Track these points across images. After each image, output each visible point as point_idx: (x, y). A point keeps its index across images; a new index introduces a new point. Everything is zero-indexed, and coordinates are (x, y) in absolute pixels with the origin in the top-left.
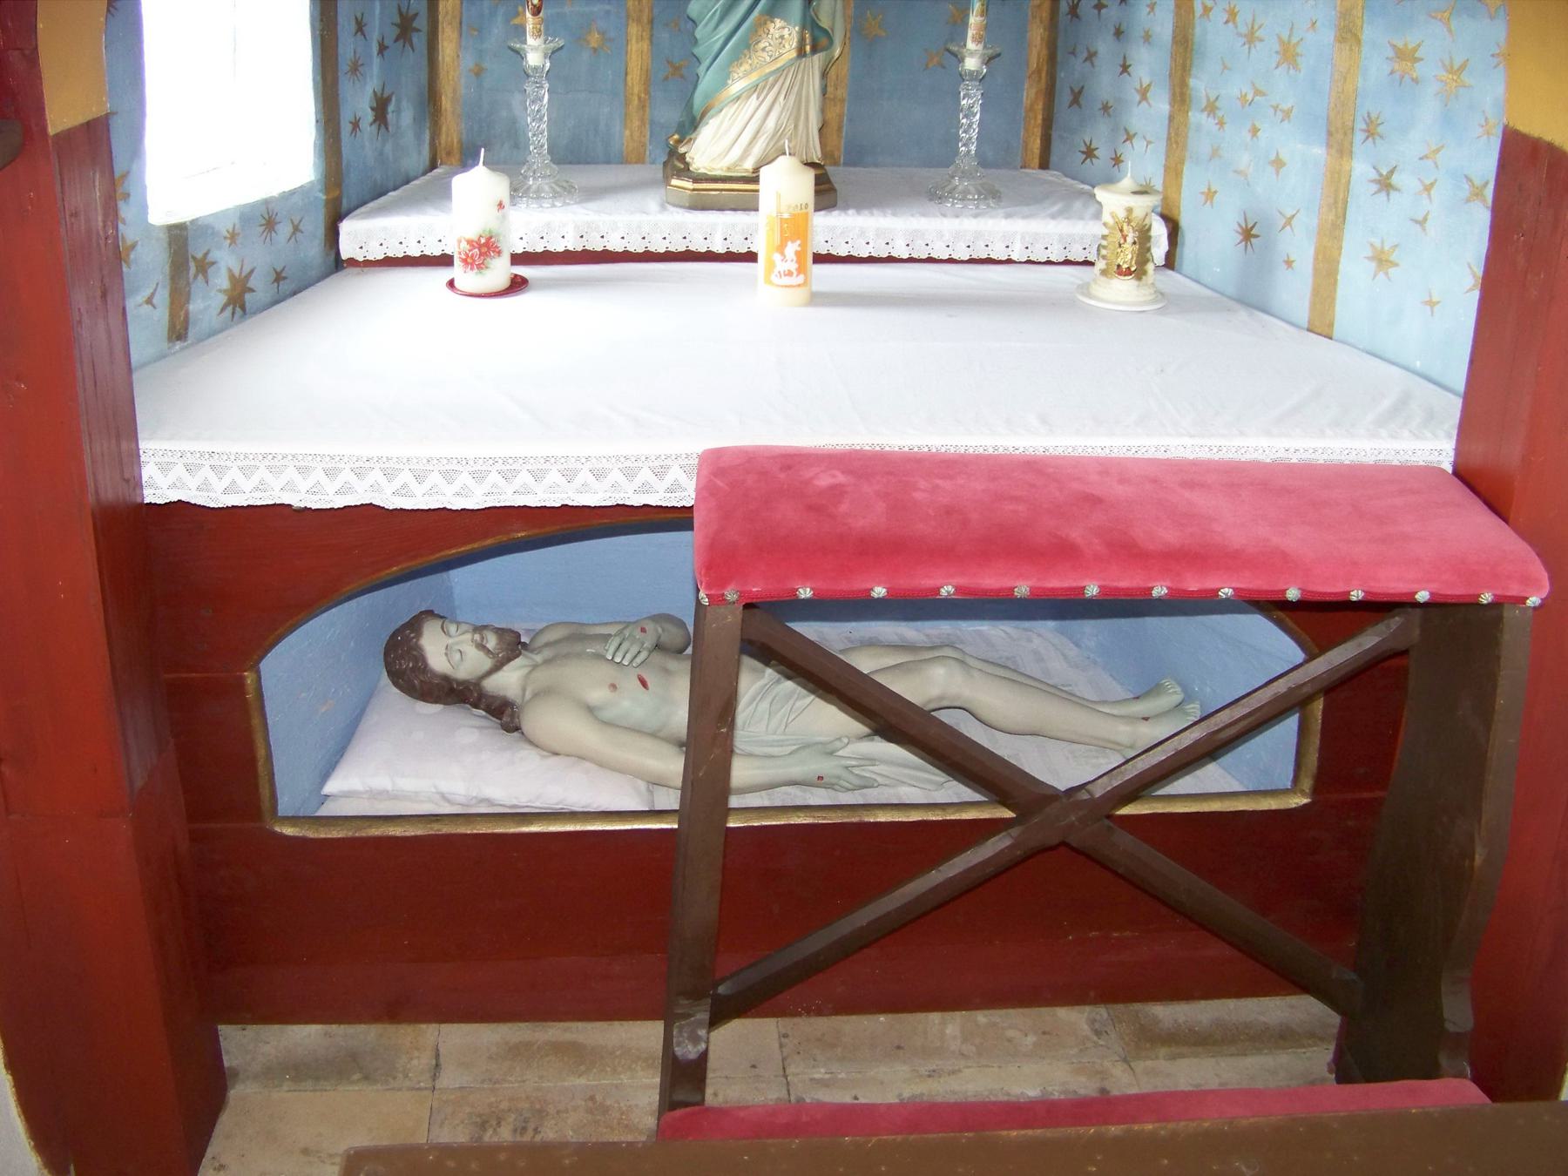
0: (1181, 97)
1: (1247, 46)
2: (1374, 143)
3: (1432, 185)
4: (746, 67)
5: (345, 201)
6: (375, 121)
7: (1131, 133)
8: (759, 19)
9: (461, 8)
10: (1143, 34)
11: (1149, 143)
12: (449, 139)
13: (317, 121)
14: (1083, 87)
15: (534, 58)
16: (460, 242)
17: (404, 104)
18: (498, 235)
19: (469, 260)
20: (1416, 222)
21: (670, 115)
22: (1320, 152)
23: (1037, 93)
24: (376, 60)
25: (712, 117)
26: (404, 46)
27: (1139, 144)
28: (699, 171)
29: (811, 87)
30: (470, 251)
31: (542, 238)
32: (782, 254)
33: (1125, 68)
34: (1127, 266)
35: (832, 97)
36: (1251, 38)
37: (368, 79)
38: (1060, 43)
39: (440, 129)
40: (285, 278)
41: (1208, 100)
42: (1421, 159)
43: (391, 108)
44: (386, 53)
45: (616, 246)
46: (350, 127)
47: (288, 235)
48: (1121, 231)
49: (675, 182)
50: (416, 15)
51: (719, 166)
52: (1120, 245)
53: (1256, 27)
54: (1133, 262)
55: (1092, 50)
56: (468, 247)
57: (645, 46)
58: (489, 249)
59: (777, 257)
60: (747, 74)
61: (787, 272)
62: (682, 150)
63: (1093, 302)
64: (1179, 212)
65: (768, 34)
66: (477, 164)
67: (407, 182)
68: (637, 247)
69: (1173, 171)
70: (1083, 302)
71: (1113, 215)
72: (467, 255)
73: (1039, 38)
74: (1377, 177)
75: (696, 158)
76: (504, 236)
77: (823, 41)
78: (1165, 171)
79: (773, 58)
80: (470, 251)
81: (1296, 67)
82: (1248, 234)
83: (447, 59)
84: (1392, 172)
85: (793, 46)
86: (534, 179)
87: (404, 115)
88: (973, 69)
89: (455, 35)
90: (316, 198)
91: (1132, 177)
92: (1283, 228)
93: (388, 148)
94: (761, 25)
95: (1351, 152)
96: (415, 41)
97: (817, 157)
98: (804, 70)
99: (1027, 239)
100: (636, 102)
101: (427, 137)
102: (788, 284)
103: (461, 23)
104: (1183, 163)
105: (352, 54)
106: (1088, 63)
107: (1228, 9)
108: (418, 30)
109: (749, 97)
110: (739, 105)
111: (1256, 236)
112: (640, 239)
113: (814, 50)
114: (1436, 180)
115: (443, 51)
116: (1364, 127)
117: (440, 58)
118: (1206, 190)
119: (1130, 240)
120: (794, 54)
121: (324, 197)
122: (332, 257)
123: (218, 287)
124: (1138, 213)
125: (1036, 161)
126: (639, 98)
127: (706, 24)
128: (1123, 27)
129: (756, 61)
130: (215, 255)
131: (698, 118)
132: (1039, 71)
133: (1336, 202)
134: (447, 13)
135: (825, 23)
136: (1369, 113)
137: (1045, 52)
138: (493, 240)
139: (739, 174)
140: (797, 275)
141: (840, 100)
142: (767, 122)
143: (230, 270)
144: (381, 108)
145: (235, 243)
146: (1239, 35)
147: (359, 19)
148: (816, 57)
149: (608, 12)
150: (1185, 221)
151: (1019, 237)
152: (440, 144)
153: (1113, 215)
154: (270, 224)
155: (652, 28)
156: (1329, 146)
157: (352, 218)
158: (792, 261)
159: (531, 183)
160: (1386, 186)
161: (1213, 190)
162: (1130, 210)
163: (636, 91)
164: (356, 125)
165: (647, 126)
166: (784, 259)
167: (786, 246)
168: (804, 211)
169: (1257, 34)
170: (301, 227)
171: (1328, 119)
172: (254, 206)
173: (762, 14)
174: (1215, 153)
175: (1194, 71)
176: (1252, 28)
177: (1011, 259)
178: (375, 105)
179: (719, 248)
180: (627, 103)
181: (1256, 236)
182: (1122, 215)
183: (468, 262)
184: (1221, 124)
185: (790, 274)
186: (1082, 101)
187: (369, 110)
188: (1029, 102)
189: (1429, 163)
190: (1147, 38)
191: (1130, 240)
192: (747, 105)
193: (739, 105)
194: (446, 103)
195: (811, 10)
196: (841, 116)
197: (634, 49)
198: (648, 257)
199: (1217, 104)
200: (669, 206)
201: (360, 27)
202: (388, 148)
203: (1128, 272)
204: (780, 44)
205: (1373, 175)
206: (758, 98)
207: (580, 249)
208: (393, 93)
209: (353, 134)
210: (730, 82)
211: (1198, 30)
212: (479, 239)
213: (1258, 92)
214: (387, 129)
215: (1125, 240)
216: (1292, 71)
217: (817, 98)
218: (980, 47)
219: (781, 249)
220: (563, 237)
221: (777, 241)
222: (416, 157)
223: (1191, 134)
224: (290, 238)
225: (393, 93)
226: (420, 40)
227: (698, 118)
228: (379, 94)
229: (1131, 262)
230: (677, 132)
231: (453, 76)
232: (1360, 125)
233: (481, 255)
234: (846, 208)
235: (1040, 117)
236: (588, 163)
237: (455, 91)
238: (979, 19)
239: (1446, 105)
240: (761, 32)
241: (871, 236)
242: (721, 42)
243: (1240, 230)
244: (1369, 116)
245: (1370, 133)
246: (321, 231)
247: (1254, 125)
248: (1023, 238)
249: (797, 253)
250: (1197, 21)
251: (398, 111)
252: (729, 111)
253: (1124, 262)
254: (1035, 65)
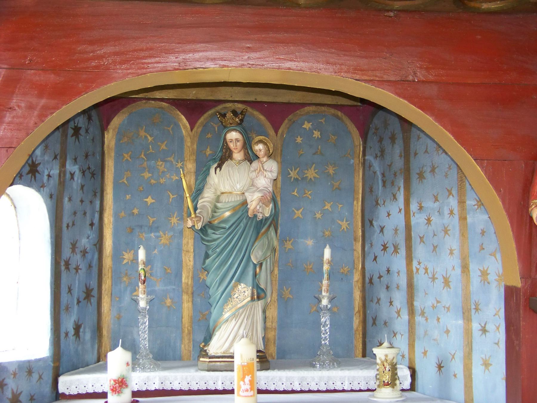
0: (412, 312)
1: (432, 282)
2: (478, 313)
3: (499, 326)
4: (230, 306)
5: (61, 369)
6: (74, 335)
7: (395, 333)
8: (235, 284)
9: (112, 287)
10: (396, 286)
11: (402, 335)
12: (106, 349)
13: (51, 329)
14: (376, 316)
15: (142, 304)
16: (110, 381)
17: (87, 330)
18: (126, 378)
19: (114, 389)
20: (496, 344)
21: (200, 337)
22: (461, 322)
23: (359, 322)
24: (76, 307)
25: (217, 332)
26: (87, 302)
27: (398, 336)
28: (212, 355)
29: (258, 316)
30: (115, 385)
31: (145, 384)
32: (244, 381)
33: (391, 303)
34: (387, 381)
35: (271, 327)
36: (434, 278)
37: (72, 314)
38: (367, 297)
39: (102, 344)
40: (34, 399)
41: (421, 310)
42: (494, 316)
43: (81, 330)
44: (80, 304)
45: (177, 387)
46: (64, 335)
47: (37, 379)
48: (384, 365)
49: (201, 359)
50: (93, 289)
51: (220, 352)
52: (384, 372)
53: (435, 273)
54: (390, 379)
55: (379, 298)
56: (114, 383)
57: (190, 304)
58: (123, 384)
59: (242, 383)
60: (230, 309)
61: (246, 390)
62: (205, 348)
63: (375, 399)
64: (415, 364)
65: (238, 291)
66: (118, 346)
67: (88, 366)
68: (185, 388)
69: (411, 346)
70: (372, 400)
71: (380, 359)
72: (113, 387)
73: (358, 296)
74: (481, 328)
75: (211, 350)
76: (129, 379)
77: (262, 294)
78: (409, 346)
79: (241, 301)
80: (115, 385)
81: (450, 288)
82: (440, 367)
83: (105, 311)
84: (485, 324)
85: (249, 296)
86: (143, 360)
87: (87, 335)
88: (325, 304)
89: (109, 300)
90: (49, 364)
91: (388, 341)
92: (452, 360)
93: (80, 348)
94: (235, 286)
95: (471, 319)
96: (92, 301)
97: (262, 349)
98: (254, 308)
99: (350, 380)
100: (186, 331)
101: (96, 346)
102: (247, 395)
103: (111, 294)
104: (415, 341)
105: (66, 302)
106: (378, 304)
107: (424, 267)
108: (94, 297)
109: (232, 320)
110: (228, 325)
111: (443, 367)
112: (187, 384)
113: (259, 298)
114: (500, 324)
115: (104, 307)
116: (474, 307)
117: (103, 311)
118: (424, 351)
119: (387, 369)
120: (249, 299)
121: (53, 365)
123: (7, 397)
124: (390, 357)
125: (361, 355)
126: (188, 329)
127: (213, 287)
128: (389, 285)
129: (234, 303)
130: (7, 381)
131: (212, 333)
132: (359, 312)
133: (468, 343)
134: (106, 290)
135: (262, 286)
136: (475, 301)
137: (361, 303)
138: (124, 380)
139: (228, 355)
140: (251, 391)
141: (274, 328)
142: (239, 331)
143: (12, 390)
144: (77, 328)
145: (15, 377)
146: (430, 278)
147: (70, 287)
148: (260, 302)
149: (174, 289)
150: (417, 368)
151: (347, 378)
152: (102, 351)
153: (380, 359)
154: (30, 372)
155: (193, 297)
156: (464, 319)
157: (64, 375)
158: (248, 384)
159: (141, 361)
160: (484, 331)
161: (426, 350)
162: (386, 356)
163: (186, 326)
164: (67, 334)
165: (192, 343)
166: (245, 384)
167: (245, 377)
168: (252, 362)
169: (435, 277)
170: (42, 377)
171: (462, 307)
172: (24, 362)
173: (236, 281)
174: (426, 333)
175: (415, 298)
176: (434, 274)
177: (344, 389)
178: (75, 327)
179: (220, 387)
180: (183, 332)
181: (443, 367)
182: (383, 358)
183: (114, 390)
184: (427, 319)
185: (247, 390)
186: (377, 322)
187: (72, 329)
188: (356, 326)
189: (497, 316)
190: (398, 287)
191: (387, 369)
192: (231, 324)
193: (228, 325)
194: (105, 332)
195: (256, 280)
196: (274, 336)
197: (185, 306)
198: (190, 392)
199: (424, 311)
200: (198, 370)
201: (70, 290)
202: (80, 348)
203: (388, 384)
204: (244, 295)
205: (480, 328)
206: (235, 320)
207: (161, 389)
208: (82, 323)
209: (65, 339)
210: (224, 313)
211: (415, 280)
212: (119, 379)
213: (438, 302)
214: (79, 339)
215: (385, 369)
216: (448, 289)
217: (261, 321)
218: (328, 294)
219: (243, 379)
220: (154, 383)
221: (242, 377)
222: (92, 356)
223: (417, 327)
224: (38, 381)
225: (82, 323)
226: (94, 300)
227: (212, 333)
228: (77, 322)
229: (389, 380)
230: (204, 342)
231: (108, 320)
232: (473, 307)
233: (119, 387)
234: (274, 369)
235: (361, 333)
236: (166, 360)
237: (108, 327)
238: (326, 282)
239: (499, 290)
240: (235, 290)
241: (284, 380)
242: (219, 296)
243: (437, 366)
244: (475, 302)
245: (477, 309)
246: (50, 381)
247: (438, 317)
248: (348, 379)
249: (250, 381)
250: (415, 275)
251: (84, 332)
252: (223, 327)
253: (386, 380)
254: (357, 309)
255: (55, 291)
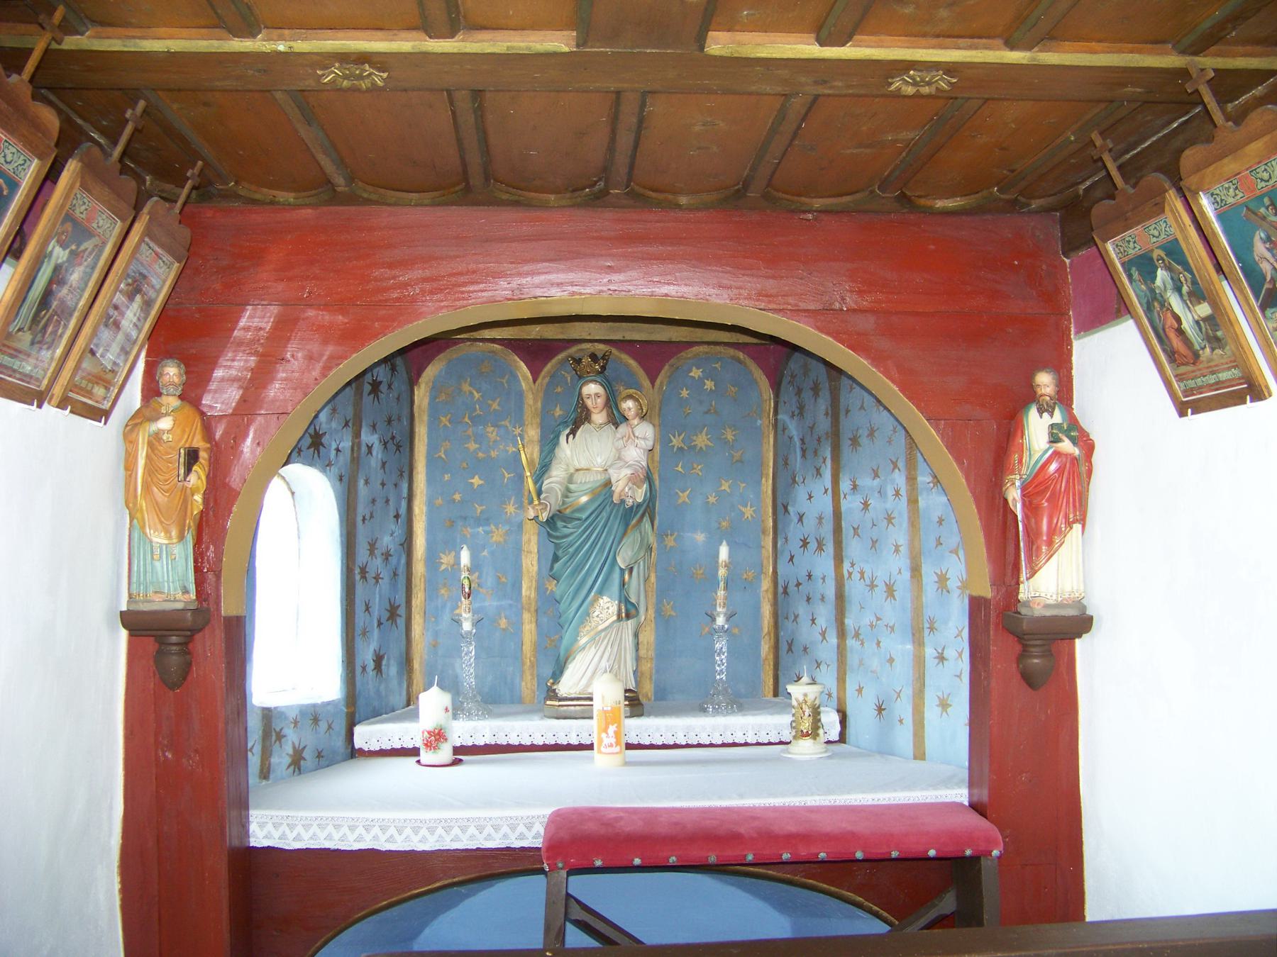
0: (842, 634)
5: (357, 715)
6: (375, 669)
11: (828, 666)
16: (423, 733)
17: (392, 662)
18: (445, 728)
21: (548, 671)
24: (376, 631)
27: (823, 667)
33: (813, 620)
36: (872, 586)
38: (780, 612)
43: (384, 662)
44: (382, 626)
49: (548, 702)
50: (399, 606)
59: (604, 735)
60: (588, 632)
62: (555, 687)
63: (790, 756)
69: (841, 680)
71: (797, 700)
77: (633, 611)
82: (880, 709)
89: (421, 621)
94: (595, 600)
96: (398, 621)
100: (528, 663)
101: (405, 686)
108: (400, 616)
109: (590, 648)
111: (884, 709)
113: (628, 616)
119: (807, 714)
120: (615, 618)
122: (350, 747)
124: (810, 698)
125: (772, 693)
132: (769, 633)
135: (633, 600)
137: (772, 621)
144: (378, 660)
148: (629, 622)
149: (511, 605)
150: (849, 712)
153: (797, 700)
156: (914, 642)
162: (805, 695)
163: (528, 656)
164: (364, 668)
174: (861, 663)
179: (574, 741)
180: (523, 664)
181: (884, 709)
182: (801, 699)
183: (428, 745)
184: (862, 644)
185: (611, 745)
190: (823, 599)
191: (807, 714)
194: (416, 665)
203: (807, 735)
207: (493, 743)
211: (847, 588)
213: (878, 619)
219: (606, 730)
221: (604, 727)
222: (398, 698)
223: (849, 655)
230: (551, 678)
232: (926, 625)
233: (436, 740)
234: (649, 715)
235: (772, 663)
237: (421, 657)
238: (722, 592)
240: (595, 606)
242: (573, 612)
245: (931, 629)
246: (343, 732)
248: (753, 728)
249: (615, 732)
251: (388, 665)
252: (579, 657)
255: (347, 609)
